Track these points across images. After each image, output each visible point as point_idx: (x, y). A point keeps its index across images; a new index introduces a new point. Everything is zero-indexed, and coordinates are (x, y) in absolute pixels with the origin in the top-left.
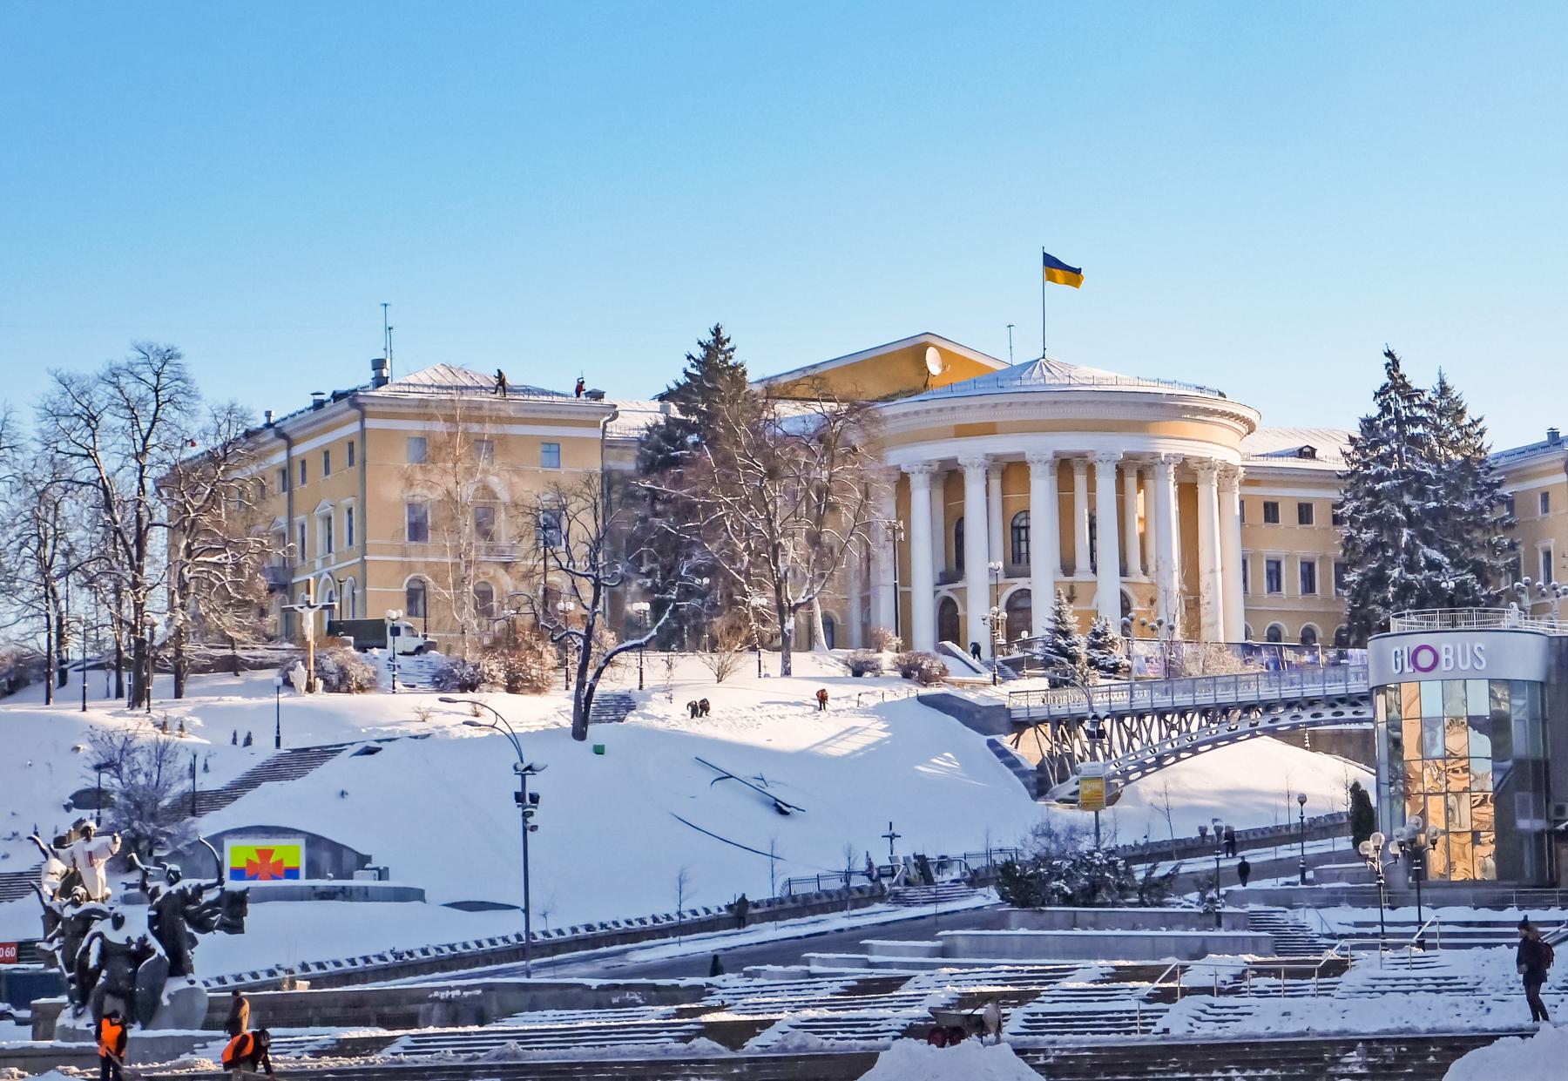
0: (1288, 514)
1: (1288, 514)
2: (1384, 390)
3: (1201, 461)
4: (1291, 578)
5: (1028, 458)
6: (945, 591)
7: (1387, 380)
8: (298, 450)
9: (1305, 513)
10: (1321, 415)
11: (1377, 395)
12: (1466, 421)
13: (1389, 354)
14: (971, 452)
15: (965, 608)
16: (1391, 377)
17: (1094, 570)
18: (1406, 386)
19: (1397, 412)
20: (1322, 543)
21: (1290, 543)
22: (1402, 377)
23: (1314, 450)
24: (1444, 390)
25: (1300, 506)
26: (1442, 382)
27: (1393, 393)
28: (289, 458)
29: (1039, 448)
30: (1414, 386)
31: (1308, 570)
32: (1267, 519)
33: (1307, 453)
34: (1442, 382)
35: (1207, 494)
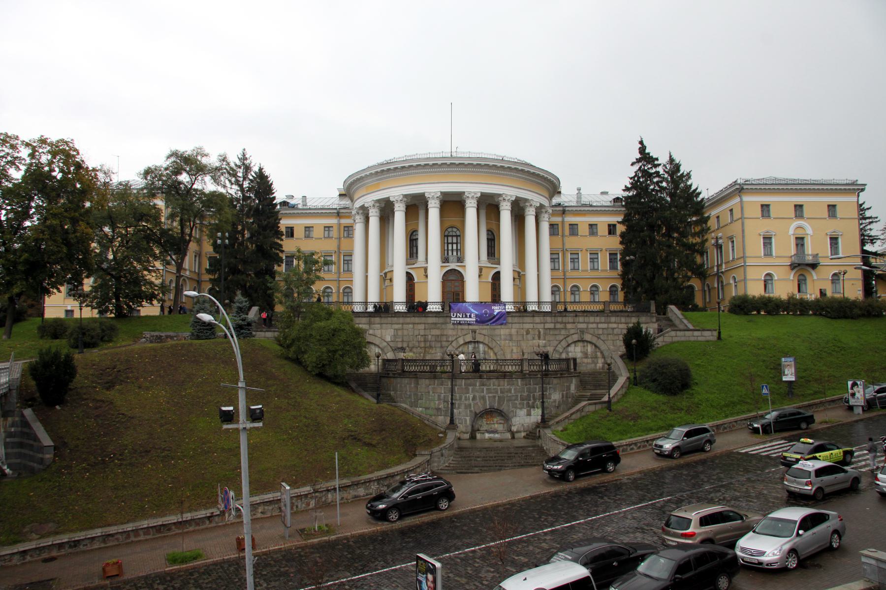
1: (603, 230)
2: (638, 161)
4: (604, 261)
5: (392, 199)
7: (639, 156)
9: (612, 229)
11: (632, 164)
13: (641, 143)
16: (640, 153)
22: (649, 154)
24: (671, 160)
25: (609, 225)
26: (670, 156)
30: (654, 157)
31: (613, 255)
34: (670, 156)
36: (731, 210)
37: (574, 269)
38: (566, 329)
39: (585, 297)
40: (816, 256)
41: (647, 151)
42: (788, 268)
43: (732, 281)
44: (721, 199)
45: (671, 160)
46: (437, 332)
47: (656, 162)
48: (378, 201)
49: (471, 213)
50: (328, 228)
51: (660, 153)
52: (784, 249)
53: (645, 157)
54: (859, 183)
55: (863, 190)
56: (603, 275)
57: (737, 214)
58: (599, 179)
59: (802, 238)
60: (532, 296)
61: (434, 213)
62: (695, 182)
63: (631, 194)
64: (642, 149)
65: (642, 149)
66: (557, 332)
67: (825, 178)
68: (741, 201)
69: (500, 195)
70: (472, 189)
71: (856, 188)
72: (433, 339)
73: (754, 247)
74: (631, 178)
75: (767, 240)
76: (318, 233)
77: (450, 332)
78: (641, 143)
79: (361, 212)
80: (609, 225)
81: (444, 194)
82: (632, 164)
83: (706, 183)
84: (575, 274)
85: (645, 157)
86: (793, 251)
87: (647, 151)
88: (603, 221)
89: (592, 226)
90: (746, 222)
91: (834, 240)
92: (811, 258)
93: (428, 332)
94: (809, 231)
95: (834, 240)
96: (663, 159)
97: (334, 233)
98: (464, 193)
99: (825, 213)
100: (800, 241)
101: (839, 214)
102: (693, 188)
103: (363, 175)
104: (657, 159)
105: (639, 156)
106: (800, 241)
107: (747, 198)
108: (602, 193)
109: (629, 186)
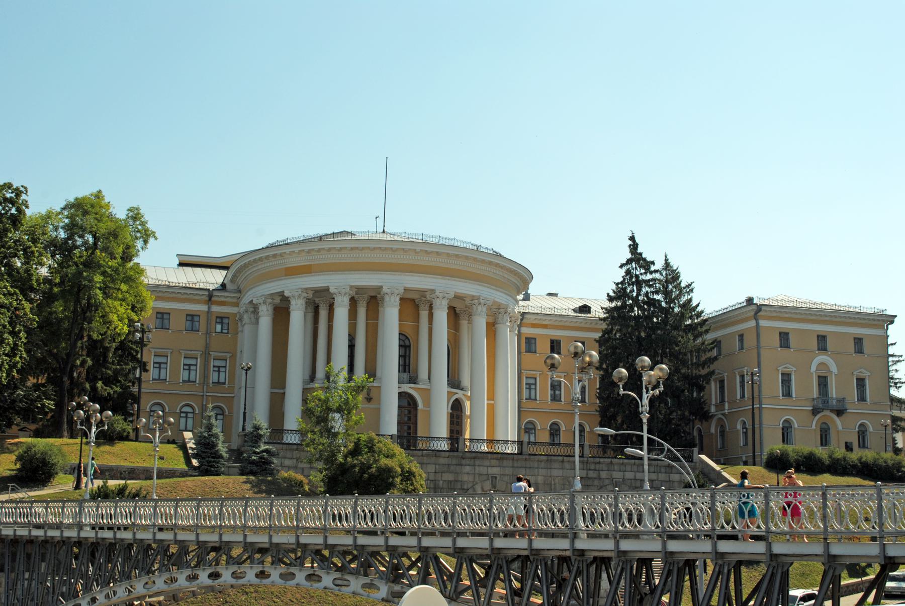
2: (629, 261)
3: (473, 298)
5: (332, 290)
7: (629, 256)
11: (621, 267)
12: (683, 285)
13: (632, 238)
18: (645, 260)
19: (637, 276)
22: (641, 254)
23: (590, 308)
24: (667, 265)
26: (666, 260)
27: (633, 264)
30: (648, 259)
33: (585, 309)
34: (666, 260)
36: (741, 336)
37: (529, 399)
38: (599, 478)
39: (545, 437)
40: (842, 400)
41: (639, 251)
42: (810, 414)
43: (739, 427)
44: (726, 318)
45: (667, 265)
46: (449, 477)
47: (653, 268)
48: (306, 290)
49: (442, 317)
50: (191, 317)
52: (806, 389)
53: (636, 257)
54: (887, 313)
55: (892, 322)
57: (750, 341)
58: (576, 280)
59: (825, 378)
60: (476, 430)
61: (391, 316)
62: (696, 298)
63: (613, 305)
64: (634, 247)
65: (634, 247)
66: (589, 483)
68: (757, 324)
72: (445, 486)
73: (772, 386)
74: (617, 284)
75: (786, 379)
76: (178, 323)
77: (465, 478)
78: (632, 238)
79: (269, 301)
81: (406, 290)
82: (621, 267)
84: (531, 404)
85: (636, 257)
86: (815, 394)
87: (639, 251)
90: (763, 352)
91: (861, 382)
92: (834, 402)
93: (439, 476)
94: (834, 368)
95: (861, 382)
96: (659, 265)
97: (203, 326)
98: (433, 291)
99: (851, 347)
100: (823, 382)
101: (866, 348)
102: (694, 303)
103: (287, 251)
104: (653, 263)
105: (629, 256)
106: (823, 382)
108: (550, 295)
109: (612, 294)
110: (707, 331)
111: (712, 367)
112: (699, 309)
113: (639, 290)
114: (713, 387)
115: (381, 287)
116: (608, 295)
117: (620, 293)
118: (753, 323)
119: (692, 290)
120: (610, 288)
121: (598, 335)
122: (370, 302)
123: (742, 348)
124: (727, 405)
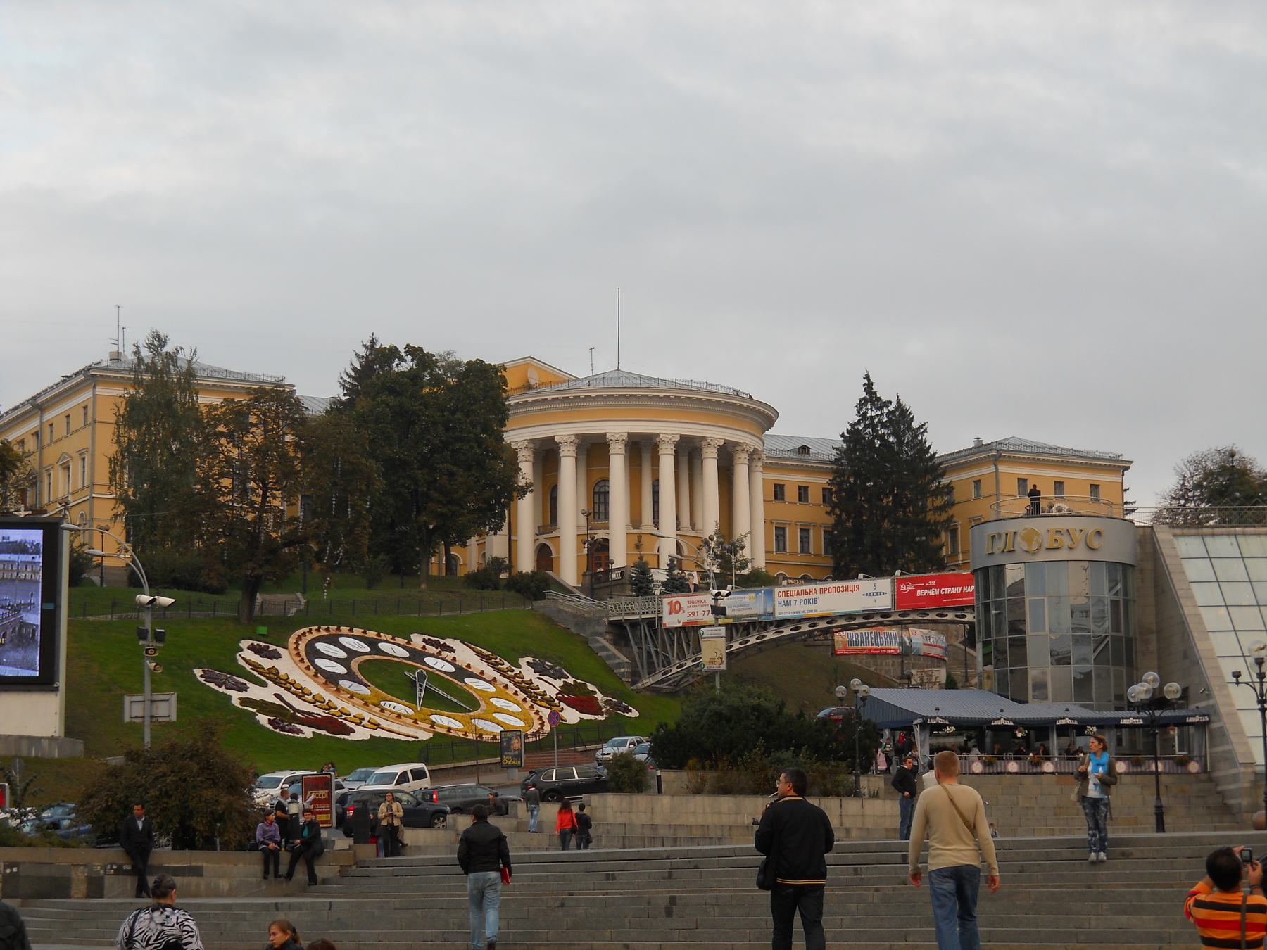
0: (791, 494)
1: (791, 494)
4: (792, 539)
5: (609, 437)
6: (542, 539)
7: (864, 395)
8: (48, 416)
9: (803, 491)
10: (818, 419)
12: (915, 425)
13: (867, 377)
14: (565, 431)
15: (558, 551)
17: (656, 524)
18: (879, 399)
20: (816, 514)
21: (792, 512)
25: (800, 487)
26: (898, 400)
28: (41, 423)
29: (617, 429)
30: (885, 399)
31: (805, 532)
32: (776, 498)
33: (804, 450)
34: (898, 400)
35: (741, 471)
36: (977, 482)
44: (961, 461)
48: (577, 435)
51: (883, 393)
53: (871, 397)
55: (1128, 468)
56: (793, 560)
57: (987, 488)
64: (868, 387)
65: (868, 387)
67: (1089, 448)
68: (997, 472)
69: (736, 444)
70: (715, 433)
71: (1119, 466)
80: (800, 487)
83: (941, 443)
85: (871, 397)
88: (792, 480)
89: (779, 492)
98: (704, 438)
99: (1087, 495)
107: (1003, 469)
110: (942, 475)
111: (950, 512)
112: (931, 451)
113: (875, 431)
114: (944, 537)
115: (658, 435)
116: (842, 435)
117: (853, 436)
118: (992, 469)
119: (925, 431)
120: (844, 428)
121: (824, 480)
122: (641, 449)
123: (978, 496)
124: (960, 556)
